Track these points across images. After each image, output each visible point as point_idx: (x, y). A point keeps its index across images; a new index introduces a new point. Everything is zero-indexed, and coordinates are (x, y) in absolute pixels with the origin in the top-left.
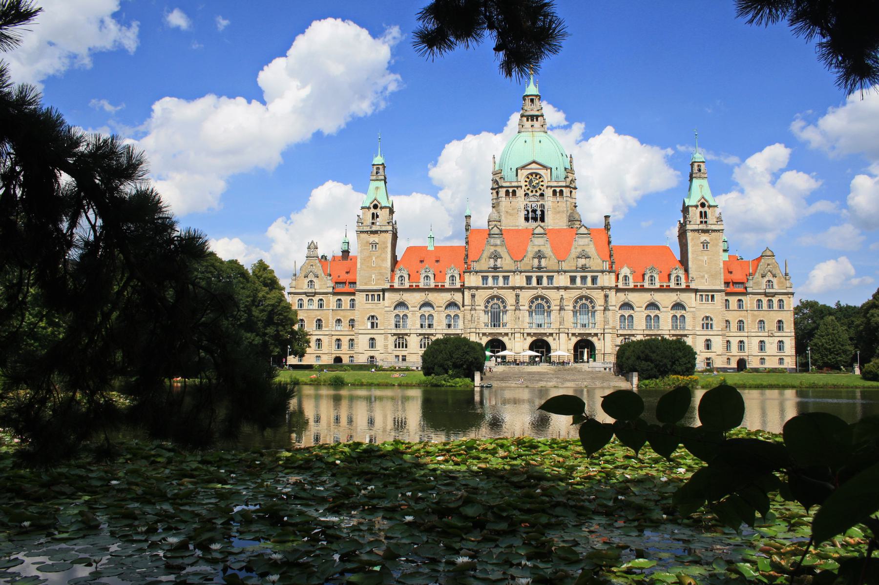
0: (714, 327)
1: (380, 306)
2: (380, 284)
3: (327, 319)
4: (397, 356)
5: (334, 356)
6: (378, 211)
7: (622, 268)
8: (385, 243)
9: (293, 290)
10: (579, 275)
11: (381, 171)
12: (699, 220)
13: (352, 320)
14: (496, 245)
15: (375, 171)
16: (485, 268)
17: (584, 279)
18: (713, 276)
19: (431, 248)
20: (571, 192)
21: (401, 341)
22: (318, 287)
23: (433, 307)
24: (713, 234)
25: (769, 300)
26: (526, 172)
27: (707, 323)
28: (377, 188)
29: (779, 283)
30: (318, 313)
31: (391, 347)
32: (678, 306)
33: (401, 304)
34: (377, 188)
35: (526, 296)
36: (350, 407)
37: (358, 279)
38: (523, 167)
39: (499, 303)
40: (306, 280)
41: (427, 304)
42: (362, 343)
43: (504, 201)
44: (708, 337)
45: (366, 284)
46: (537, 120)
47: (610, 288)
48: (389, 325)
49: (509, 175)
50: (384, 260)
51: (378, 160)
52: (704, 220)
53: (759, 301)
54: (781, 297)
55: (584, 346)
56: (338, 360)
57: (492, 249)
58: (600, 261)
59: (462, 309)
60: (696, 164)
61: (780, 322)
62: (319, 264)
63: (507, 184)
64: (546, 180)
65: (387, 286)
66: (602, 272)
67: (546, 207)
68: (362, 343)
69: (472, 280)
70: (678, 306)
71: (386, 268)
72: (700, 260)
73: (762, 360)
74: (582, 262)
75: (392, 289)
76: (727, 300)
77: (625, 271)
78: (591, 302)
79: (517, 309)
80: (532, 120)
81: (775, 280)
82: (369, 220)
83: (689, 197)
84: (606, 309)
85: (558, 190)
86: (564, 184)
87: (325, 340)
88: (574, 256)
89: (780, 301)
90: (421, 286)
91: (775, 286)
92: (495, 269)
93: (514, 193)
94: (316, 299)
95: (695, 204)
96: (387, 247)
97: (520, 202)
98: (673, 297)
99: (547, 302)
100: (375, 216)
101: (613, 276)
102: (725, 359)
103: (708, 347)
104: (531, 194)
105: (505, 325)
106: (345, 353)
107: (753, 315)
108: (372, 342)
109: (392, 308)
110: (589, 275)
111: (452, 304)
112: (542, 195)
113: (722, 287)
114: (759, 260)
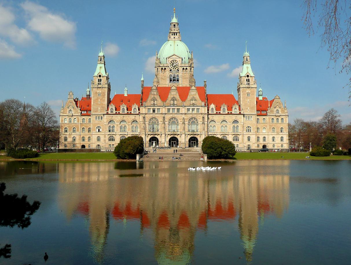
0: (251, 131)
1: (102, 122)
2: (102, 112)
3: (78, 128)
4: (110, 145)
5: (81, 144)
6: (101, 78)
7: (211, 104)
8: (104, 93)
9: (62, 114)
10: (191, 108)
11: (102, 59)
13: (89, 128)
14: (154, 95)
15: (100, 59)
16: (149, 105)
17: (193, 110)
18: (252, 108)
19: (126, 95)
22: (73, 112)
23: (126, 122)
24: (252, 89)
25: (277, 119)
26: (170, 60)
27: (249, 130)
28: (101, 67)
29: (282, 111)
30: (74, 125)
31: (107, 140)
32: (236, 121)
34: (101, 67)
35: (168, 117)
36: (89, 166)
37: (92, 109)
39: (155, 120)
40: (68, 111)
41: (123, 121)
42: (94, 138)
43: (161, 74)
44: (249, 135)
45: (96, 112)
46: (177, 34)
47: (205, 114)
48: (106, 130)
49: (163, 60)
50: (104, 101)
51: (101, 54)
52: (248, 83)
53: (273, 119)
54: (282, 117)
55: (193, 141)
56: (83, 146)
57: (152, 96)
58: (200, 101)
59: (139, 123)
60: (245, 57)
61: (282, 128)
62: (74, 102)
63: (162, 65)
64: (179, 64)
66: (202, 106)
67: (180, 76)
68: (94, 138)
69: (143, 110)
70: (236, 121)
71: (105, 104)
72: (246, 101)
73: (274, 146)
74: (194, 102)
75: (107, 114)
76: (258, 119)
77: (212, 106)
78: (197, 120)
80: (174, 35)
81: (280, 110)
82: (97, 82)
83: (242, 72)
84: (203, 123)
85: (185, 68)
86: (188, 65)
87: (77, 138)
88: (189, 100)
89: (282, 119)
90: (121, 112)
91: (280, 112)
93: (165, 69)
94: (72, 118)
95: (244, 75)
96: (105, 95)
97: (167, 73)
98: (234, 117)
99: (177, 120)
100: (100, 80)
101: (206, 108)
102: (256, 145)
103: (249, 140)
104: (173, 70)
105: (158, 130)
106: (86, 143)
107: (270, 125)
108: (99, 139)
109: (108, 123)
110: (196, 108)
112: (178, 70)
113: (255, 113)
114: (273, 100)
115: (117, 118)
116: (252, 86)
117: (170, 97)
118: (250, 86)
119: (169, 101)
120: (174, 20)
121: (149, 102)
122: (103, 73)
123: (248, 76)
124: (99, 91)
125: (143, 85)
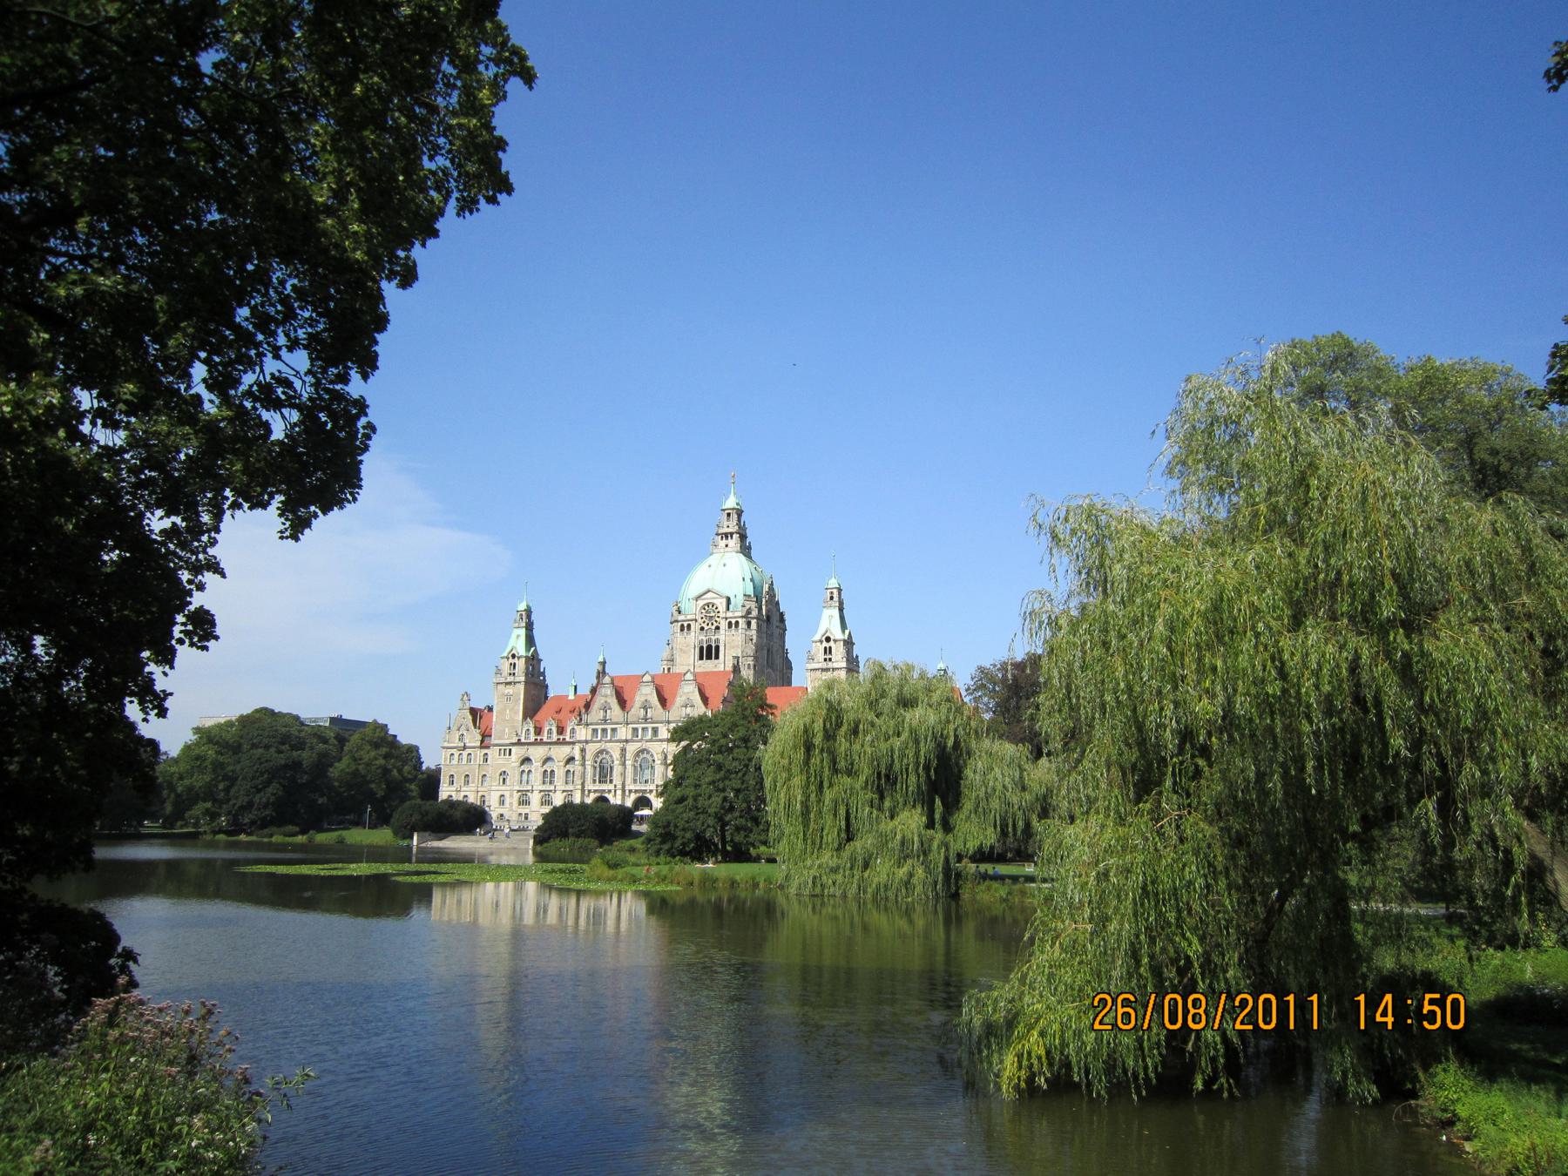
12: (821, 656)
20: (749, 624)
21: (524, 802)
26: (701, 603)
31: (515, 804)
33: (527, 760)
35: (632, 748)
38: (698, 598)
43: (680, 638)
65: (515, 740)
75: (519, 743)
79: (624, 764)
92: (605, 721)
94: (465, 753)
97: (694, 639)
111: (571, 760)
115: (537, 753)
116: (835, 665)
117: (639, 700)
118: (830, 665)
119: (636, 711)
120: (731, 503)
121: (595, 714)
122: (521, 650)
123: (828, 639)
124: (510, 690)
125: (602, 673)
